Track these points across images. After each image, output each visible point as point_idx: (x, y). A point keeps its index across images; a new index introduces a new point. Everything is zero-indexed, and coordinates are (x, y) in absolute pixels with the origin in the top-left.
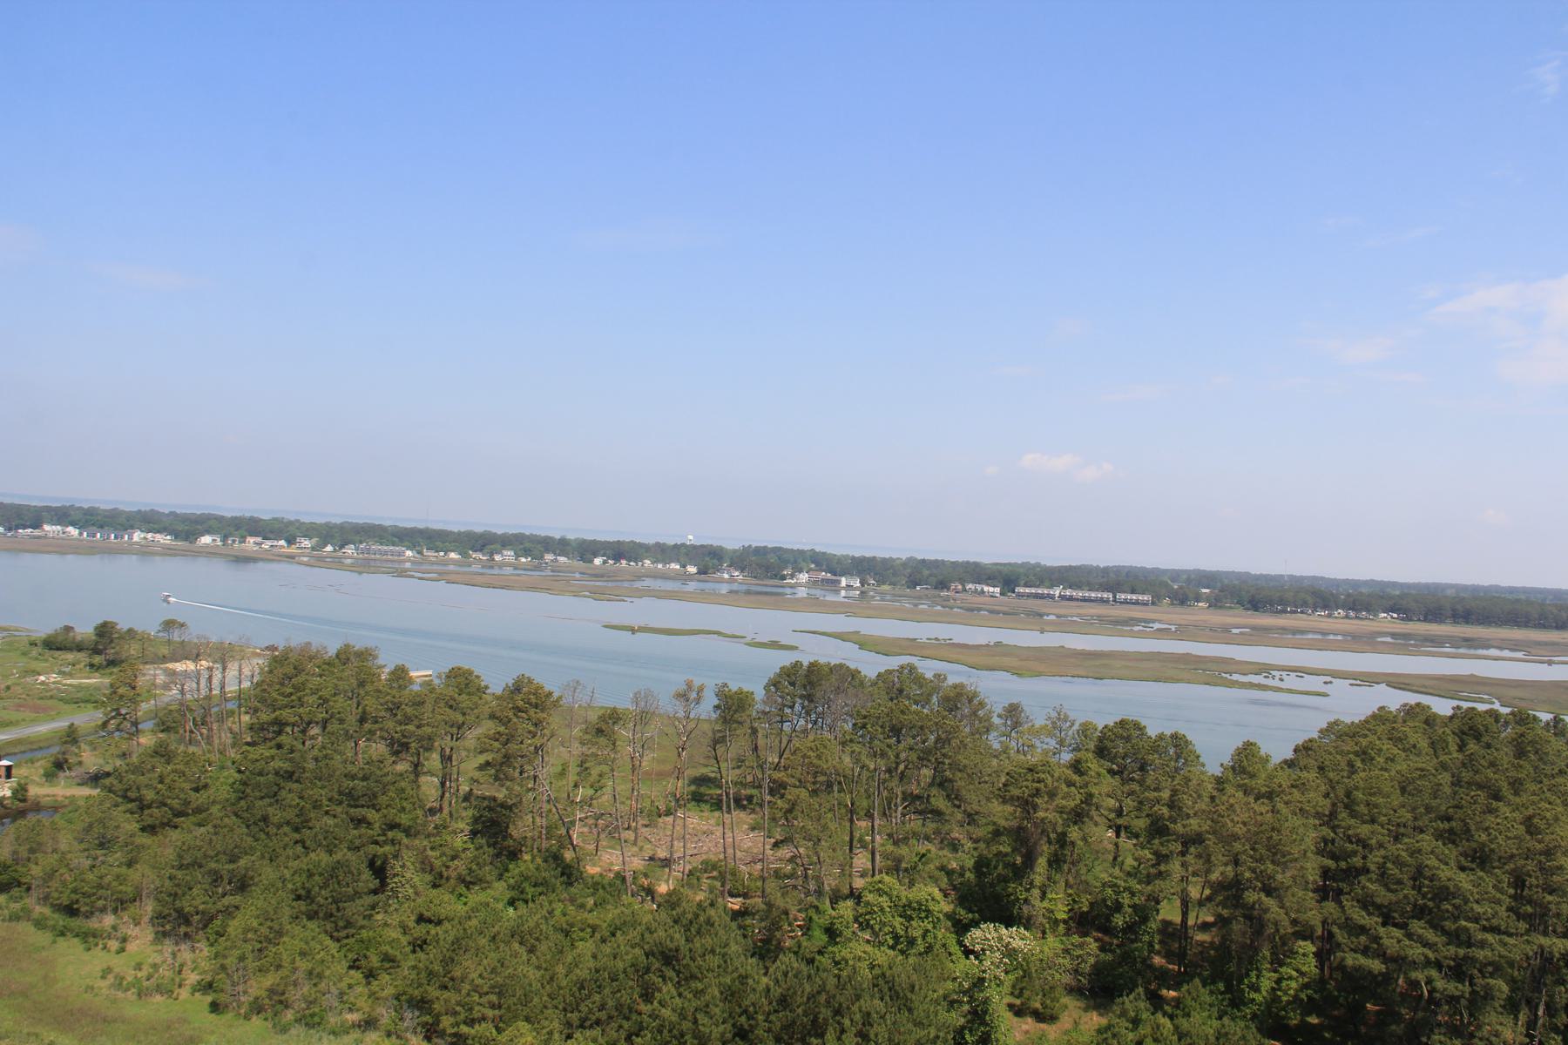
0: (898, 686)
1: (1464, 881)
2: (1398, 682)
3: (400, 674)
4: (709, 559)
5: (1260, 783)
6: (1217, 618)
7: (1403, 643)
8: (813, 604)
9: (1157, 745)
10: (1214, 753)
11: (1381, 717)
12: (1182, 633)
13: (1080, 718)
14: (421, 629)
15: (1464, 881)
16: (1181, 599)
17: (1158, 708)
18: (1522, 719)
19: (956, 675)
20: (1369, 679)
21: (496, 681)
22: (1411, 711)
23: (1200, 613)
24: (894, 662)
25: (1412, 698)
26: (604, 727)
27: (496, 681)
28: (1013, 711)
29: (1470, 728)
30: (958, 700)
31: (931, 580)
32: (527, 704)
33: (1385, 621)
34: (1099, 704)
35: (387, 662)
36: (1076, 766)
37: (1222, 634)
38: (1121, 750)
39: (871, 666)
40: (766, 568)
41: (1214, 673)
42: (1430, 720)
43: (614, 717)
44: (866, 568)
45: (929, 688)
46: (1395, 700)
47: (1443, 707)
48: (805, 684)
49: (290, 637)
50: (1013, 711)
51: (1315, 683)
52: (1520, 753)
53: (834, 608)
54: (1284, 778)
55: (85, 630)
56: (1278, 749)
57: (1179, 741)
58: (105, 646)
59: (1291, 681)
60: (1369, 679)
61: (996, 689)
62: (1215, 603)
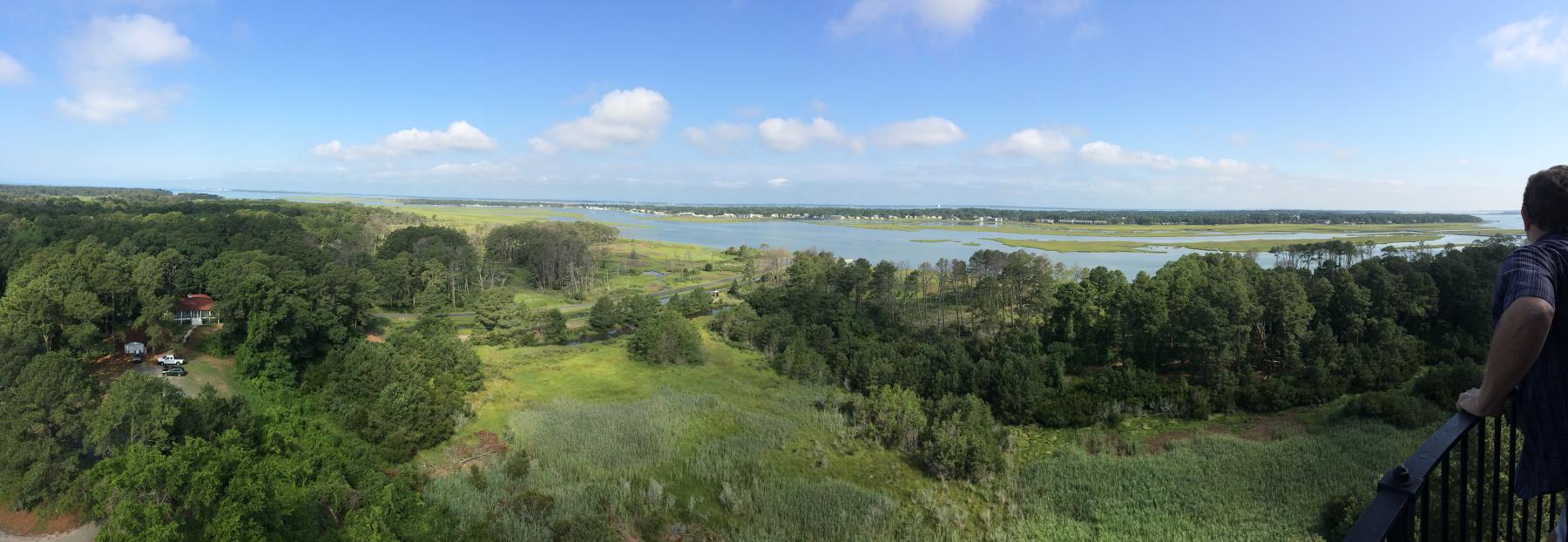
3: (842, 260)
5: (1146, 286)
7: (1189, 233)
9: (1110, 275)
10: (1130, 278)
11: (1183, 259)
12: (1117, 233)
13: (1082, 266)
17: (1111, 262)
18: (1227, 255)
19: (1039, 253)
21: (874, 263)
22: (1191, 256)
24: (1016, 249)
27: (874, 263)
29: (1210, 260)
34: (1091, 262)
35: (837, 257)
36: (1082, 284)
38: (1099, 277)
39: (1008, 250)
41: (1129, 248)
42: (1198, 258)
43: (915, 273)
44: (1007, 215)
46: (1188, 252)
47: (1202, 253)
49: (802, 248)
50: (1059, 265)
54: (1153, 284)
55: (737, 249)
57: (1118, 273)
58: (739, 255)
61: (1053, 258)
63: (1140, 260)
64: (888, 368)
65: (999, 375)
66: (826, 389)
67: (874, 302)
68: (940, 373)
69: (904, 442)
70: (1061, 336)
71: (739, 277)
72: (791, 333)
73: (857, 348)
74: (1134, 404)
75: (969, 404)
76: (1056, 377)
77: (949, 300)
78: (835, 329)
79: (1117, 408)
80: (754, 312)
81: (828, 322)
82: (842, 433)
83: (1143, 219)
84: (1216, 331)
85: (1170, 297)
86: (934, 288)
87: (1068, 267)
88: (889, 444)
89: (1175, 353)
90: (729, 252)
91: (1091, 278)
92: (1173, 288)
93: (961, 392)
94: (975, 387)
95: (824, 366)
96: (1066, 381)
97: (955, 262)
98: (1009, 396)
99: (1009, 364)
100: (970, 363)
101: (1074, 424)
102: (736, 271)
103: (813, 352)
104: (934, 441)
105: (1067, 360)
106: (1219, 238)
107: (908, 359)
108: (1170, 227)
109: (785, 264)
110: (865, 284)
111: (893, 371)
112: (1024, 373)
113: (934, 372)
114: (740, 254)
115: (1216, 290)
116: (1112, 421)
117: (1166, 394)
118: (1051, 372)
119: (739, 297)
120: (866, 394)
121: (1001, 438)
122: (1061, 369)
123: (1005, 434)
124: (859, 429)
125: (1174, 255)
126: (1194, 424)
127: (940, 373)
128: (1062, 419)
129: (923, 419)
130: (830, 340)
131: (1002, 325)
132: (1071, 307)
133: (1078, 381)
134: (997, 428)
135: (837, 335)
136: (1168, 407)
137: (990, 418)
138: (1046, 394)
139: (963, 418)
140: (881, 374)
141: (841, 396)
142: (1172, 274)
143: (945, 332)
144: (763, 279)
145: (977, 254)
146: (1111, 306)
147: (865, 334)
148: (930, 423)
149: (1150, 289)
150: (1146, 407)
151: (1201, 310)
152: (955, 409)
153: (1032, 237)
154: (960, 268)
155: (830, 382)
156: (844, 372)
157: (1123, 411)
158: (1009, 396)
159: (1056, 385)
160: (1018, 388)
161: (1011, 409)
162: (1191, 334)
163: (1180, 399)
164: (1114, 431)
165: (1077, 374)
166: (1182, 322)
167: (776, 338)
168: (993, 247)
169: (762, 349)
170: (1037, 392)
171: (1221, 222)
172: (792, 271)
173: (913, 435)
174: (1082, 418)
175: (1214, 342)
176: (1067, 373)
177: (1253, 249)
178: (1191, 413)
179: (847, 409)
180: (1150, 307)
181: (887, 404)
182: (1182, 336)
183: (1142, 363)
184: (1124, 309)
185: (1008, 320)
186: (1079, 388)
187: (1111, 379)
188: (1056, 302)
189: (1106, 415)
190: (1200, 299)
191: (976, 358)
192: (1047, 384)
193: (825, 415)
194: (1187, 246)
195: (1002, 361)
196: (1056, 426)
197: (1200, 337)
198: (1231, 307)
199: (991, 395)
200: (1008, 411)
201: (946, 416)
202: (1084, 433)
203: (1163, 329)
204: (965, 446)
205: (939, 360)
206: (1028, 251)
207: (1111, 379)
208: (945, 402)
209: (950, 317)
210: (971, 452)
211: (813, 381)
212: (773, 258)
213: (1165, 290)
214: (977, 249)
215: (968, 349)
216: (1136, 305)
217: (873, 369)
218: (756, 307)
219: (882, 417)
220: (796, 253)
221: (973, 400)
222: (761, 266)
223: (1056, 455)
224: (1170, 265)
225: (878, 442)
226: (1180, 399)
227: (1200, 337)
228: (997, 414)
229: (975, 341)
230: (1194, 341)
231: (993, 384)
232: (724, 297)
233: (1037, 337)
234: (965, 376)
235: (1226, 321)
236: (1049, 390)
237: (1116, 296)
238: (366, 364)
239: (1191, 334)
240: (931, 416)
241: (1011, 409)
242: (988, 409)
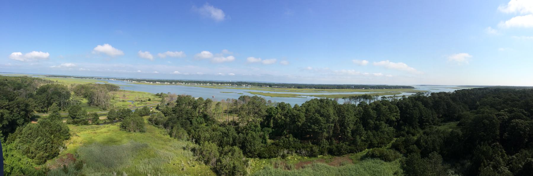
0: (255, 98)
1: (321, 118)
2: (315, 96)
3: (194, 98)
4: (233, 83)
6: (295, 89)
7: (316, 92)
8: (245, 89)
11: (312, 100)
12: (291, 91)
14: (197, 93)
15: (321, 118)
16: (290, 88)
17: (286, 101)
18: (327, 99)
19: (262, 97)
20: (311, 96)
22: (315, 99)
23: (293, 89)
25: (315, 98)
26: (218, 104)
27: (205, 99)
28: (269, 101)
29: (321, 101)
30: (262, 99)
31: (260, 85)
32: (208, 102)
33: (314, 89)
34: (280, 100)
37: (295, 91)
38: (282, 106)
40: (240, 84)
41: (294, 96)
42: (317, 100)
43: (219, 103)
45: (259, 98)
46: (313, 98)
47: (319, 98)
48: (243, 98)
50: (269, 101)
51: (305, 97)
52: (327, 103)
53: (247, 89)
55: (160, 94)
56: (300, 104)
57: (289, 104)
59: (303, 96)
60: (311, 96)
61: (267, 98)
62: (294, 88)
63: (296, 100)
64: (208, 135)
65: (246, 139)
66: (187, 143)
67: (205, 113)
68: (225, 138)
69: (211, 162)
70: (268, 126)
71: (159, 103)
72: (175, 123)
73: (198, 128)
74: (292, 151)
75: (235, 150)
76: (265, 140)
77: (231, 112)
78: (191, 121)
79: (286, 151)
80: (163, 115)
81: (188, 119)
82: (191, 159)
83: (299, 87)
84: (322, 126)
85: (306, 113)
86: (225, 108)
87: (273, 101)
88: (206, 163)
89: (309, 133)
90: (157, 95)
91: (279, 106)
92: (307, 110)
93: (232, 145)
94: (237, 144)
95: (186, 134)
96: (269, 141)
97: (233, 100)
98: (249, 147)
99: (250, 135)
100: (237, 135)
101: (270, 157)
102: (159, 101)
103: (183, 129)
104: (221, 162)
105: (270, 134)
106: (326, 94)
107: (215, 133)
108: (309, 89)
109: (175, 99)
110: (202, 106)
111: (209, 136)
112: (254, 138)
113: (223, 137)
114: (161, 95)
115: (322, 111)
116: (283, 157)
117: (303, 148)
118: (264, 138)
119: (159, 110)
120: (199, 144)
121: (246, 163)
122: (267, 137)
123: (247, 161)
124: (196, 157)
125: (309, 99)
126: (313, 159)
127: (225, 138)
128: (267, 155)
129: (218, 154)
130: (189, 125)
131: (248, 121)
132: (272, 116)
133: (272, 141)
134: (244, 159)
135: (191, 123)
136: (304, 152)
137: (242, 155)
138: (262, 146)
139: (232, 155)
140: (205, 137)
141: (192, 145)
142: (308, 104)
143: (229, 124)
144: (168, 104)
145: (241, 97)
146: (285, 115)
147: (201, 123)
148: (220, 156)
149: (299, 110)
150: (296, 152)
151: (316, 118)
152: (230, 151)
153: (262, 91)
154: (236, 103)
155: (188, 140)
156: (193, 137)
157: (288, 153)
158: (249, 147)
159: (265, 143)
160: (252, 144)
161: (250, 152)
162: (313, 126)
163: (308, 149)
164: (284, 160)
165: (273, 139)
166: (310, 122)
167: (171, 124)
168: (245, 94)
169: (165, 128)
170: (258, 145)
171: (327, 88)
172: (177, 101)
173: (214, 160)
174: (273, 154)
175: (321, 129)
176: (270, 138)
177: (337, 97)
178: (312, 155)
179: (193, 150)
180: (298, 116)
181: (206, 148)
182: (310, 127)
183: (295, 136)
184: (290, 116)
185: (251, 120)
186: (273, 144)
187: (284, 141)
188: (267, 114)
189: (281, 154)
190: (316, 114)
191: (238, 133)
192: (262, 142)
193: (186, 151)
194: (315, 96)
195: (247, 134)
196: (265, 158)
197: (316, 127)
198: (328, 117)
199: (243, 147)
200: (248, 152)
201: (226, 154)
202: (273, 160)
203: (303, 125)
204: (232, 165)
205: (225, 133)
206: (259, 96)
207: (284, 141)
208: (226, 148)
209: (231, 118)
210: (234, 167)
211: (182, 140)
212: (172, 97)
213: (304, 111)
214: (241, 95)
215: (236, 130)
216: (294, 116)
217: (202, 136)
218: (165, 114)
219: (204, 153)
220: (179, 96)
221: (236, 148)
222: (167, 100)
223: (264, 168)
224: (307, 102)
225: (203, 162)
226: (308, 149)
227: (316, 127)
228: (245, 153)
229: (238, 127)
230: (314, 129)
231: (244, 142)
232: (154, 110)
233: (259, 126)
234: (234, 140)
235: (325, 122)
236: (263, 145)
237: (287, 112)
238: (30, 131)
239: (313, 126)
240: (221, 153)
241: (250, 152)
242: (241, 152)
